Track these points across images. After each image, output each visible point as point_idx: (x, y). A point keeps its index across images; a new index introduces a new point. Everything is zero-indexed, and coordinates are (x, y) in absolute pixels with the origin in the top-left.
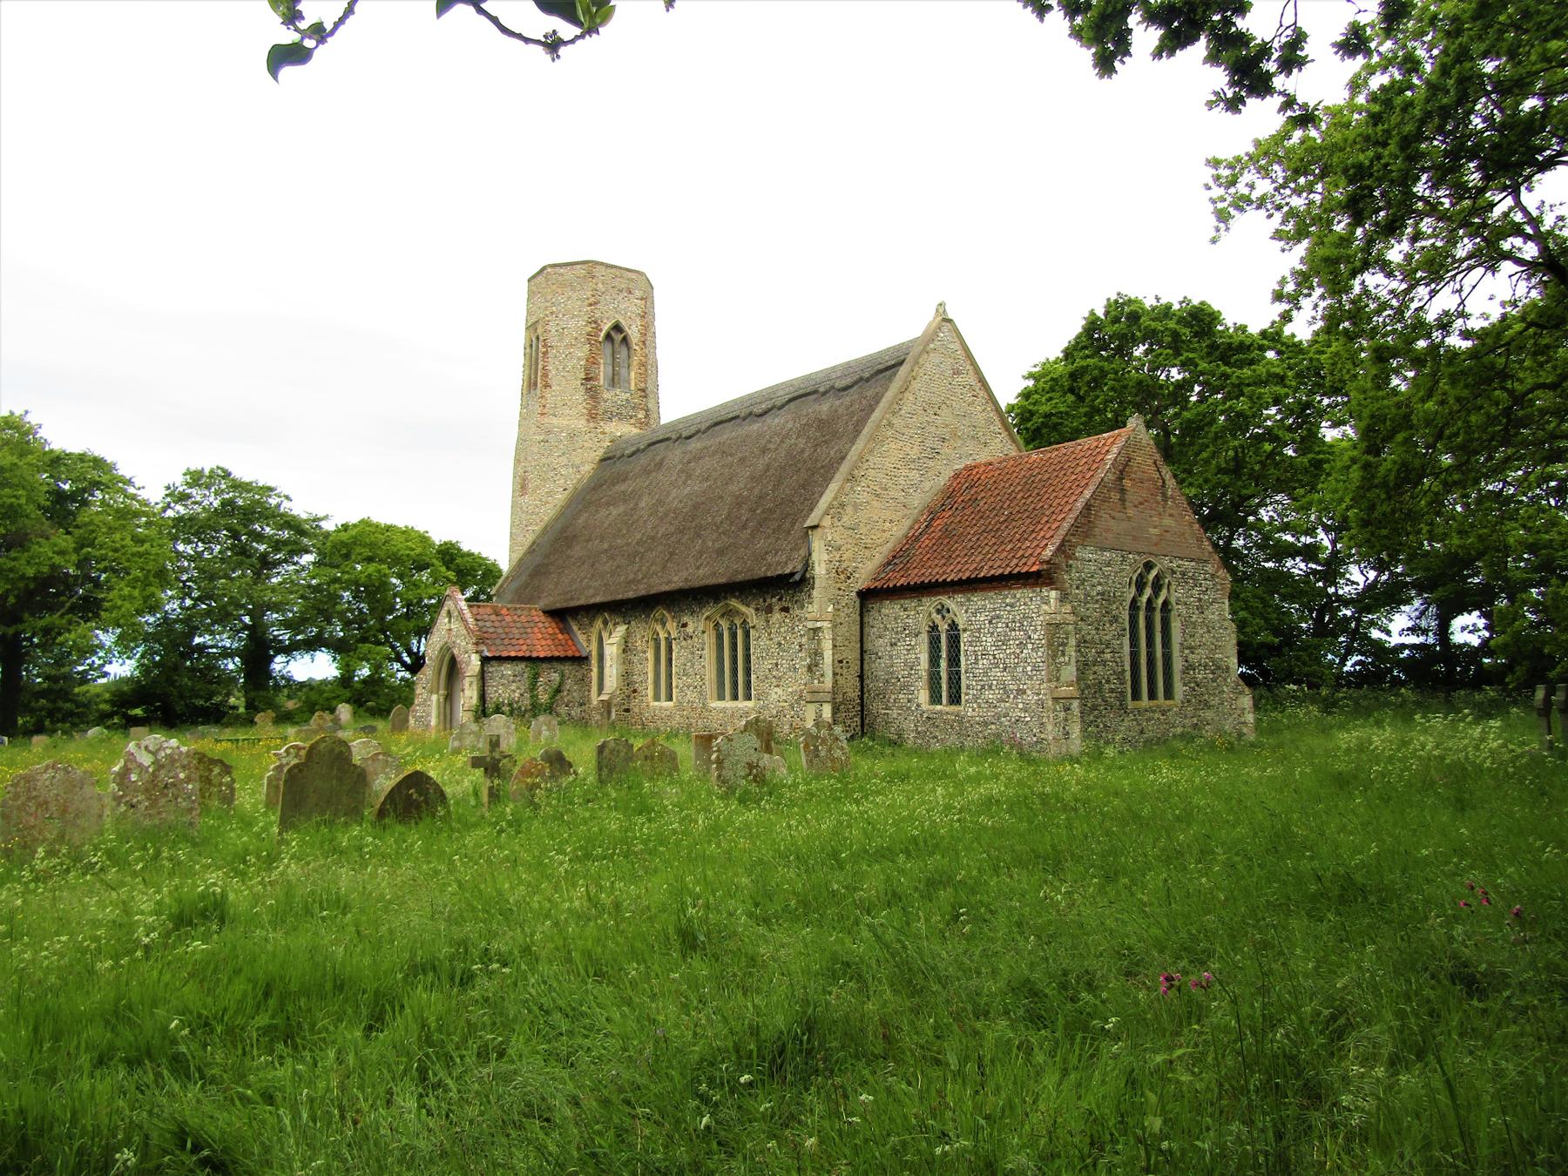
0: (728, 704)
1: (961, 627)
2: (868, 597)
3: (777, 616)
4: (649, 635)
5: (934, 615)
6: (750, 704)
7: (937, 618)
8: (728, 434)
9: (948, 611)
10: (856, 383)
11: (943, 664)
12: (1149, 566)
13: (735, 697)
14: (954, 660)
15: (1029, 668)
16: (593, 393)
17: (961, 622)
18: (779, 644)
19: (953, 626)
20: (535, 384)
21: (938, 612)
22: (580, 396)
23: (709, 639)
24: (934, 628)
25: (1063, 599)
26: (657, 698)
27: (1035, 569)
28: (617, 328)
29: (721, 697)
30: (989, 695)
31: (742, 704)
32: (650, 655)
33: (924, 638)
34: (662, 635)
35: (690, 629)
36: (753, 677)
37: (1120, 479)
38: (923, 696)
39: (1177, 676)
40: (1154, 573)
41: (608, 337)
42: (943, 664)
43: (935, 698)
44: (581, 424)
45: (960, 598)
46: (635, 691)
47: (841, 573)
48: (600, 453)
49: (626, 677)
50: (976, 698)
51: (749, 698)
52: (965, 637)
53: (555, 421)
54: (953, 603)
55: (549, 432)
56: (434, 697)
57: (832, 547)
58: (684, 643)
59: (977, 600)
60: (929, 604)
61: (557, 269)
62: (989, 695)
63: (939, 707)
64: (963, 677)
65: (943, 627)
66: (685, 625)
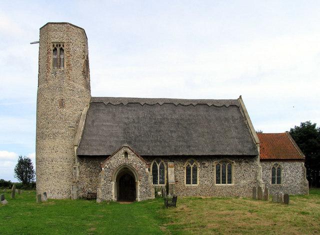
3: (243, 164)
4: (185, 166)
6: (232, 184)
8: (180, 111)
10: (222, 106)
13: (224, 182)
22: (82, 77)
24: (274, 168)
26: (188, 182)
29: (218, 182)
34: (192, 166)
35: (207, 164)
38: (271, 183)
43: (273, 182)
54: (280, 163)
56: (113, 183)
58: (203, 169)
59: (286, 163)
60: (273, 163)
65: (276, 168)
66: (205, 164)
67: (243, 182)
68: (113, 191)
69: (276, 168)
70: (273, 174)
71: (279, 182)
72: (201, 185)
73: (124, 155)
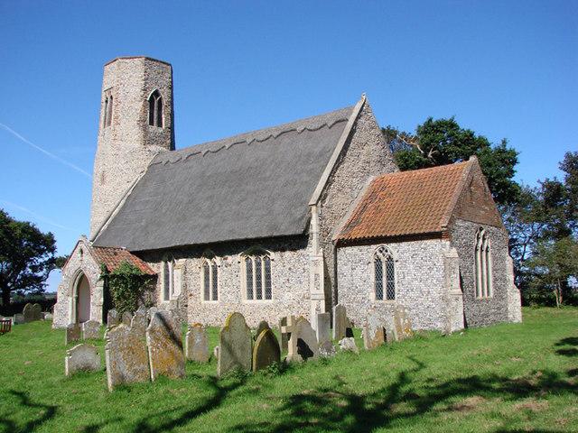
0: (255, 301)
1: (395, 259)
2: (341, 244)
5: (379, 254)
7: (380, 255)
9: (387, 251)
11: (384, 279)
12: (481, 229)
13: (259, 297)
14: (390, 276)
15: (435, 281)
16: (145, 129)
17: (395, 257)
18: (290, 269)
19: (390, 259)
20: (110, 123)
21: (381, 252)
23: (243, 266)
24: (378, 260)
25: (452, 246)
26: (207, 298)
27: (437, 230)
28: (156, 94)
30: (411, 294)
31: (264, 301)
32: (202, 274)
33: (372, 266)
36: (273, 287)
37: (470, 186)
38: (372, 296)
39: (491, 284)
40: (483, 232)
41: (152, 97)
42: (384, 279)
43: (379, 296)
44: (137, 145)
45: (393, 245)
46: (191, 295)
47: (325, 232)
48: (148, 162)
49: (185, 287)
50: (404, 296)
51: (269, 297)
52: (396, 265)
53: (123, 144)
54: (391, 247)
55: (119, 149)
56: (70, 299)
57: (321, 218)
59: (404, 245)
61: (125, 60)
62: (411, 294)
63: (381, 302)
64: (396, 285)
65: (384, 260)
67: (288, 297)
68: (70, 313)
69: (384, 260)
70: (378, 276)
71: (391, 296)
72: (223, 304)
73: (80, 255)
